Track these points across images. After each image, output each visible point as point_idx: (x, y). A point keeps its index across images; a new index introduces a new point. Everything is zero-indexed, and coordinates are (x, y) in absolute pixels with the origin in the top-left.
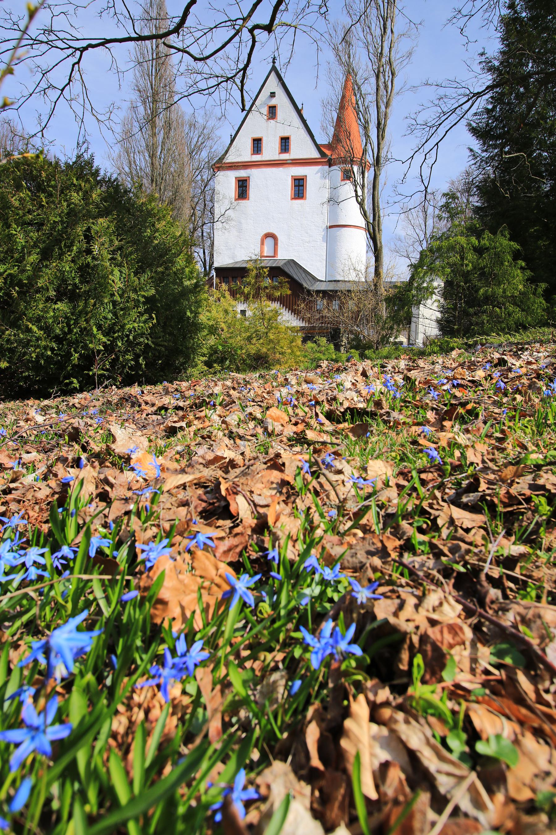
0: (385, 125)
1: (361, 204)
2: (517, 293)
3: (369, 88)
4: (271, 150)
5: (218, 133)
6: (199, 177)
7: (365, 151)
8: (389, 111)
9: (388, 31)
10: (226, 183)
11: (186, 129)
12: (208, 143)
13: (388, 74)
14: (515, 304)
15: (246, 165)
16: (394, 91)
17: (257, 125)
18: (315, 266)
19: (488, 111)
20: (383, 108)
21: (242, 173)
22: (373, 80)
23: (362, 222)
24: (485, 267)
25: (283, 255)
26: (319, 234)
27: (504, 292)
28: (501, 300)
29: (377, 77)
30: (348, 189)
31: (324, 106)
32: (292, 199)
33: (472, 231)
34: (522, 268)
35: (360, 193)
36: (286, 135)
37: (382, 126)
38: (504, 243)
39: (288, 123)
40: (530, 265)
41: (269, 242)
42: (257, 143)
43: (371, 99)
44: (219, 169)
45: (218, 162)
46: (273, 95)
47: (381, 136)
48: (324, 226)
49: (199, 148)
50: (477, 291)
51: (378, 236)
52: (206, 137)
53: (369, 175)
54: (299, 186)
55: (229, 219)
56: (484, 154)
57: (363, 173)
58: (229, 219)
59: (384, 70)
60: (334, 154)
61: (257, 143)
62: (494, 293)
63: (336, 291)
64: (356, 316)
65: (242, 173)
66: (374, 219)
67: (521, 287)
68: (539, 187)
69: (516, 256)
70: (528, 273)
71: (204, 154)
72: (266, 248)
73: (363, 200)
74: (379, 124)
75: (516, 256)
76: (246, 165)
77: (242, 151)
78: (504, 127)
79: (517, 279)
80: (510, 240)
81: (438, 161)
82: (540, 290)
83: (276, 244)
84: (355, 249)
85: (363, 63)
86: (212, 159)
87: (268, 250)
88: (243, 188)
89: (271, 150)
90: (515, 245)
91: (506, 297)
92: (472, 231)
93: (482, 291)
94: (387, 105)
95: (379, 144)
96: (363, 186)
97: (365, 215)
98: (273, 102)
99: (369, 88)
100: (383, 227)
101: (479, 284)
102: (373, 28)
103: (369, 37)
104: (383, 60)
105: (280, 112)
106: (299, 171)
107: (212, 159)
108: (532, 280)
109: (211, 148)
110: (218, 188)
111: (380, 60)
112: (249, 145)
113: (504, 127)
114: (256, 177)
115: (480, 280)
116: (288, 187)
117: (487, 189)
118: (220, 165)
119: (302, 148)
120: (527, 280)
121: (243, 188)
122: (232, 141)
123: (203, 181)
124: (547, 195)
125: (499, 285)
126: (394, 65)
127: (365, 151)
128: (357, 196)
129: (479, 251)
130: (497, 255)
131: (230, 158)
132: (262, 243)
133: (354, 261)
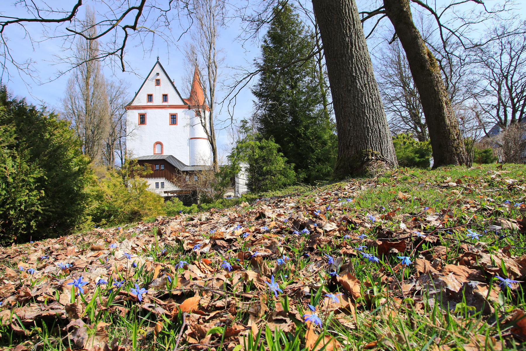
0: (214, 90)
1: (204, 127)
2: (281, 169)
3: (205, 72)
4: (158, 100)
5: (127, 91)
6: (117, 113)
7: (205, 102)
8: (215, 83)
9: (212, 49)
10: (133, 116)
11: (109, 88)
12: (122, 96)
13: (214, 67)
14: (281, 174)
15: (144, 107)
16: (217, 75)
17: (150, 87)
18: (183, 157)
19: (260, 85)
20: (212, 82)
21: (142, 111)
22: (207, 69)
23: (206, 136)
24: (264, 156)
25: (166, 153)
26: (185, 141)
27: (275, 168)
28: (274, 172)
29: (209, 68)
30: (198, 120)
31: (183, 80)
33: (259, 139)
34: (282, 156)
35: (203, 121)
37: (212, 90)
38: (273, 144)
39: (166, 88)
40: (286, 155)
41: (158, 146)
42: (150, 97)
43: (206, 78)
44: (129, 109)
45: (128, 105)
47: (212, 95)
49: (116, 97)
50: (262, 168)
51: (214, 142)
52: (120, 93)
53: (207, 113)
54: (174, 118)
55: (135, 135)
56: (260, 104)
57: (204, 112)
58: (135, 135)
59: (211, 66)
60: (191, 103)
61: (150, 97)
62: (270, 168)
63: (193, 171)
64: (205, 184)
65: (142, 111)
66: (211, 134)
67: (283, 165)
68: (286, 119)
69: (279, 151)
70: (286, 159)
71: (120, 101)
72: (156, 150)
73: (205, 125)
74: (211, 89)
75: (279, 151)
76: (144, 107)
78: (268, 92)
79: (280, 162)
80: (276, 143)
81: (240, 108)
82: (292, 167)
83: (162, 147)
84: (204, 148)
85: (202, 62)
86: (124, 104)
87: (158, 150)
88: (143, 119)
89: (158, 100)
90: (278, 146)
91: (276, 171)
92: (259, 139)
93: (265, 168)
94: (214, 81)
95: (211, 98)
96: (205, 118)
97: (207, 132)
98: (158, 78)
99: (205, 72)
100: (216, 138)
101: (263, 165)
102: (205, 46)
103: (204, 51)
104: (211, 61)
105: (162, 82)
107: (124, 104)
108: (288, 162)
109: (124, 98)
110: (128, 118)
111: (209, 61)
112: (146, 97)
113: (268, 92)
114: (150, 114)
115: (263, 163)
116: (168, 119)
117: (264, 120)
118: (129, 107)
119: (174, 100)
120: (286, 162)
121: (143, 119)
122: (136, 95)
123: (120, 115)
124: (290, 123)
125: (273, 164)
126: (216, 64)
127: (205, 102)
128: (202, 123)
129: (261, 148)
130: (270, 150)
131: (135, 104)
132: (154, 147)
133: (202, 155)
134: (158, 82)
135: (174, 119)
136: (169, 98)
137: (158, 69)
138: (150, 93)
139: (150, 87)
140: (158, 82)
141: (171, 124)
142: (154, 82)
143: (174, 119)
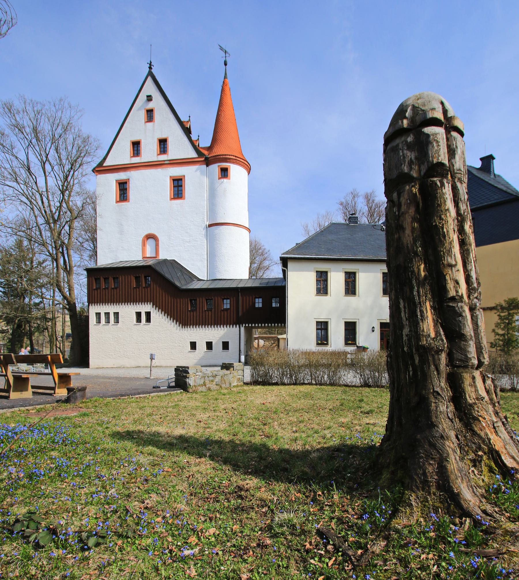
4: (150, 152)
32: (171, 199)
36: (163, 136)
46: (149, 98)
48: (204, 226)
77: (121, 155)
89: (150, 152)
98: (150, 105)
105: (157, 115)
106: (177, 171)
119: (180, 148)
134: (150, 114)
135: (178, 187)
136: (171, 145)
137: (150, 88)
138: (135, 139)
139: (137, 128)
140: (150, 114)
141: (174, 198)
142: (143, 114)
143: (178, 187)
